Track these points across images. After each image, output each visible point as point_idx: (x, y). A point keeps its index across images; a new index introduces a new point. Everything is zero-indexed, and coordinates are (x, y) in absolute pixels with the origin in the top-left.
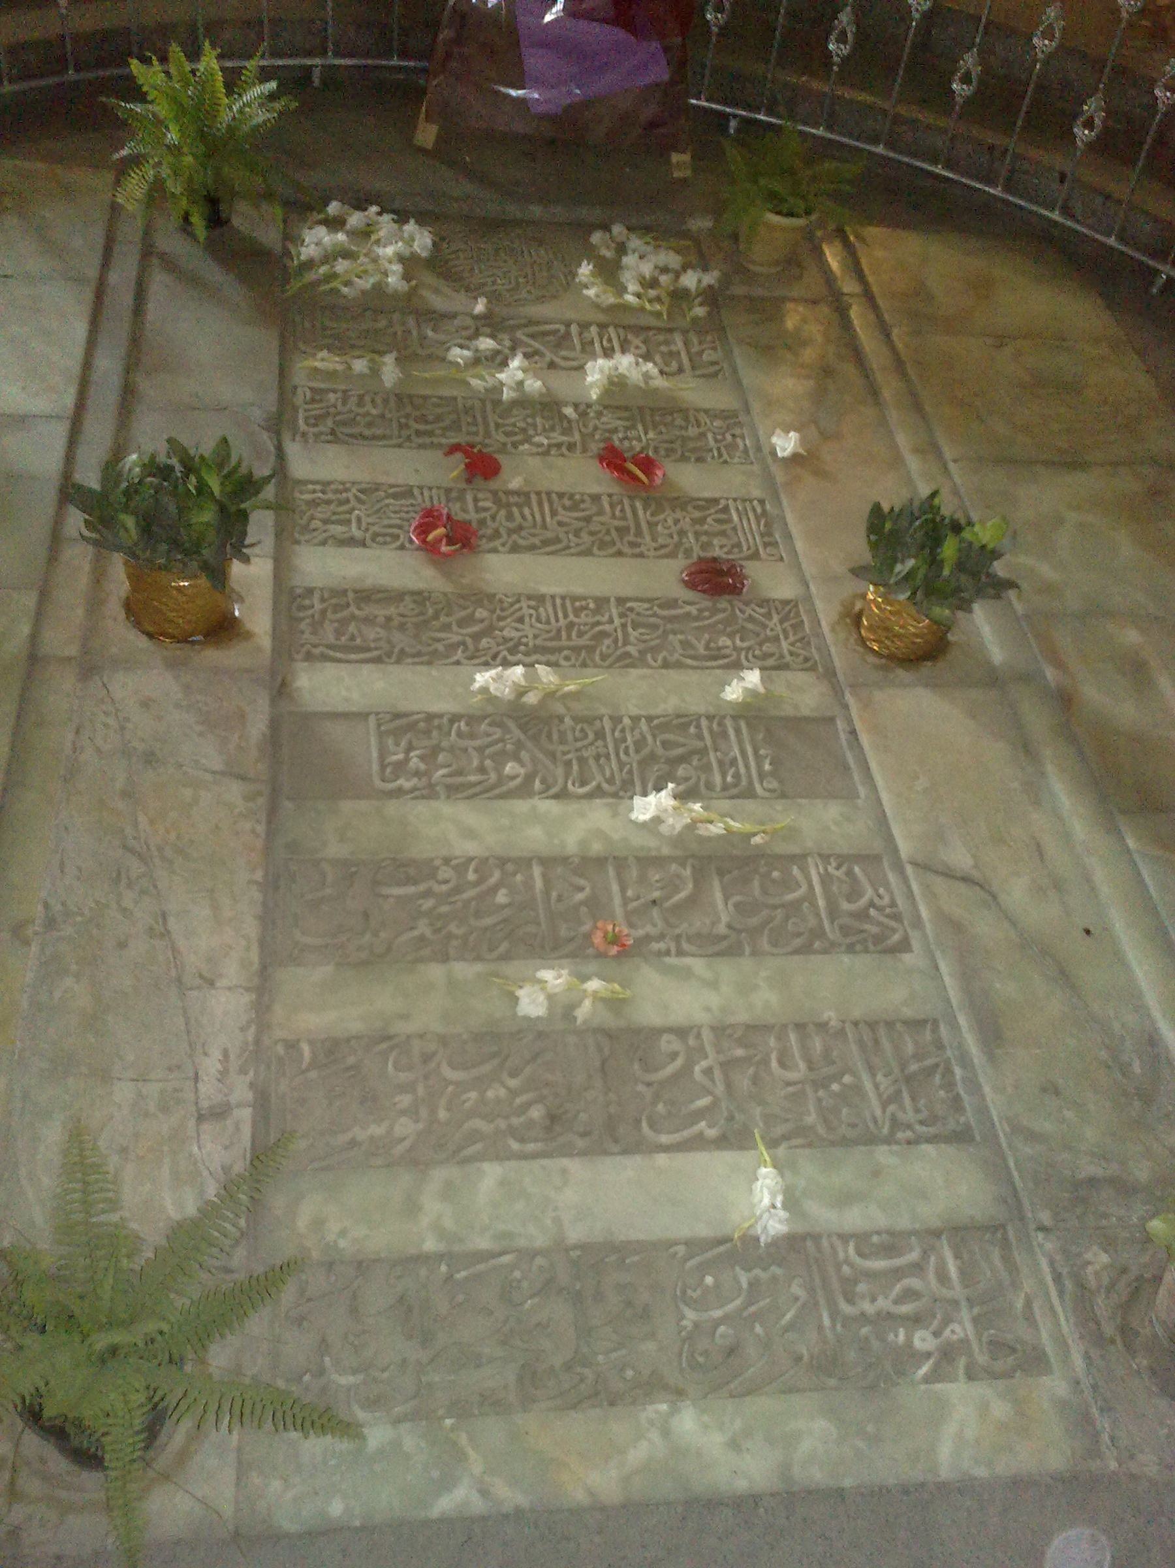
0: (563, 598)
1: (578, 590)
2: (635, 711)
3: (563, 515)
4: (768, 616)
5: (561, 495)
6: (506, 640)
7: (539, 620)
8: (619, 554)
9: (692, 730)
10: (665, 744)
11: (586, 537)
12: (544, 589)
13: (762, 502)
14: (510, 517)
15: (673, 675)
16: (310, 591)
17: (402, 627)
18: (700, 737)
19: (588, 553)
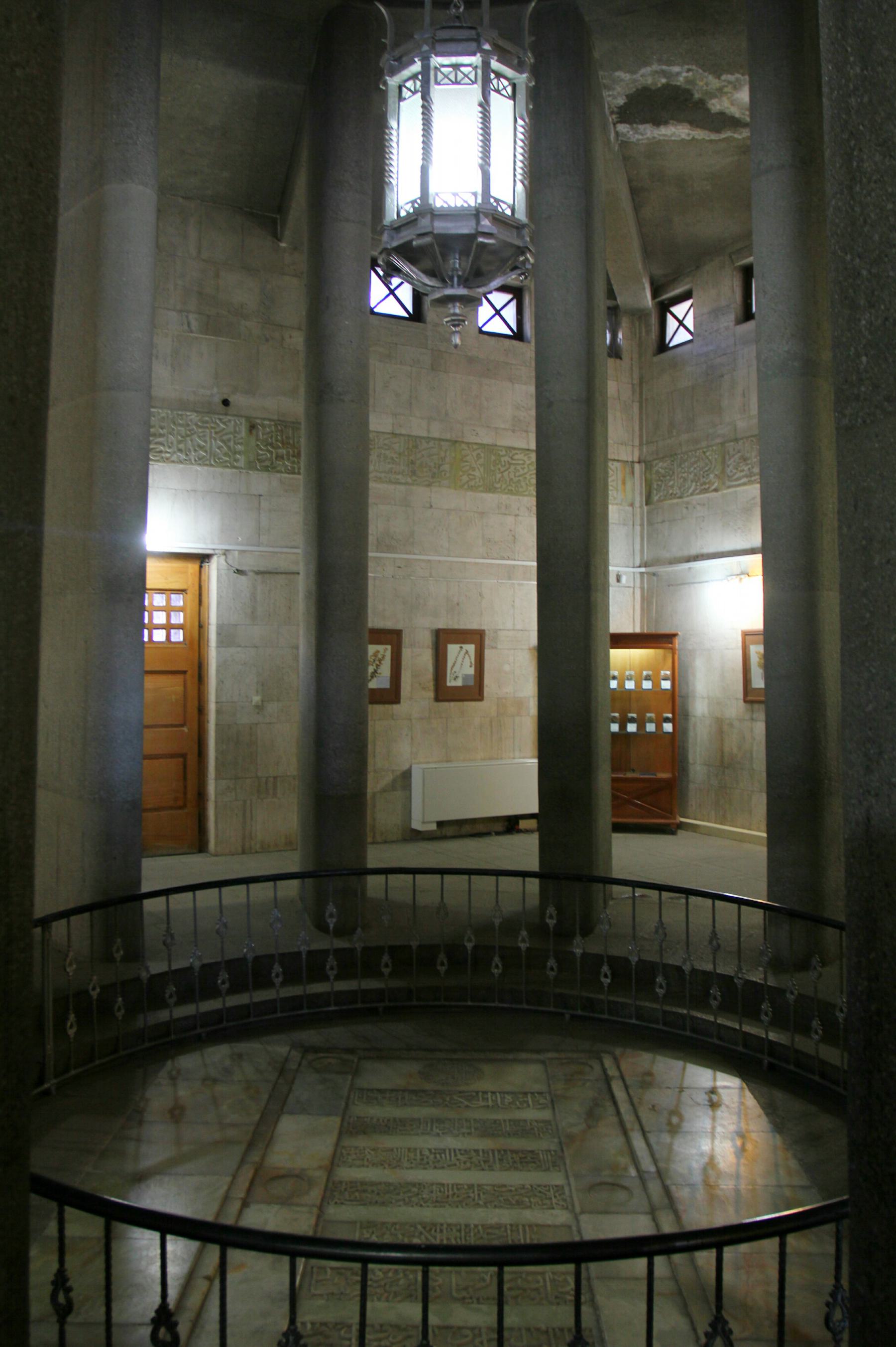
0: (453, 1185)
1: (461, 1182)
2: (476, 1222)
3: (459, 1156)
4: (549, 1190)
5: (460, 1150)
6: (423, 1199)
7: (440, 1191)
8: (483, 1170)
9: (503, 1229)
10: (488, 1234)
11: (468, 1164)
12: (444, 1182)
13: (555, 1151)
14: (435, 1158)
15: (497, 1210)
16: (341, 1182)
17: (378, 1194)
18: (506, 1231)
19: (469, 1169)
